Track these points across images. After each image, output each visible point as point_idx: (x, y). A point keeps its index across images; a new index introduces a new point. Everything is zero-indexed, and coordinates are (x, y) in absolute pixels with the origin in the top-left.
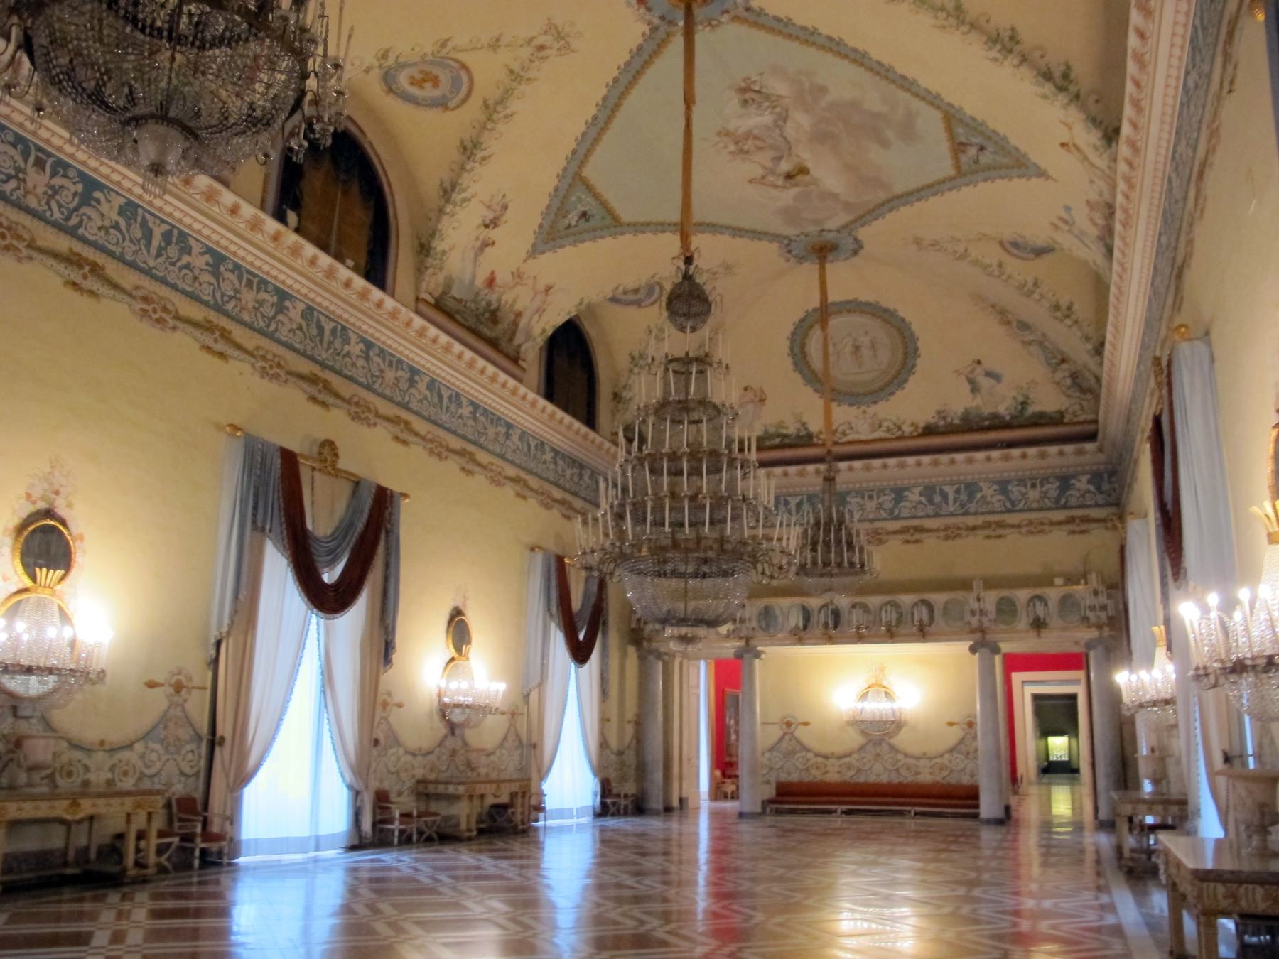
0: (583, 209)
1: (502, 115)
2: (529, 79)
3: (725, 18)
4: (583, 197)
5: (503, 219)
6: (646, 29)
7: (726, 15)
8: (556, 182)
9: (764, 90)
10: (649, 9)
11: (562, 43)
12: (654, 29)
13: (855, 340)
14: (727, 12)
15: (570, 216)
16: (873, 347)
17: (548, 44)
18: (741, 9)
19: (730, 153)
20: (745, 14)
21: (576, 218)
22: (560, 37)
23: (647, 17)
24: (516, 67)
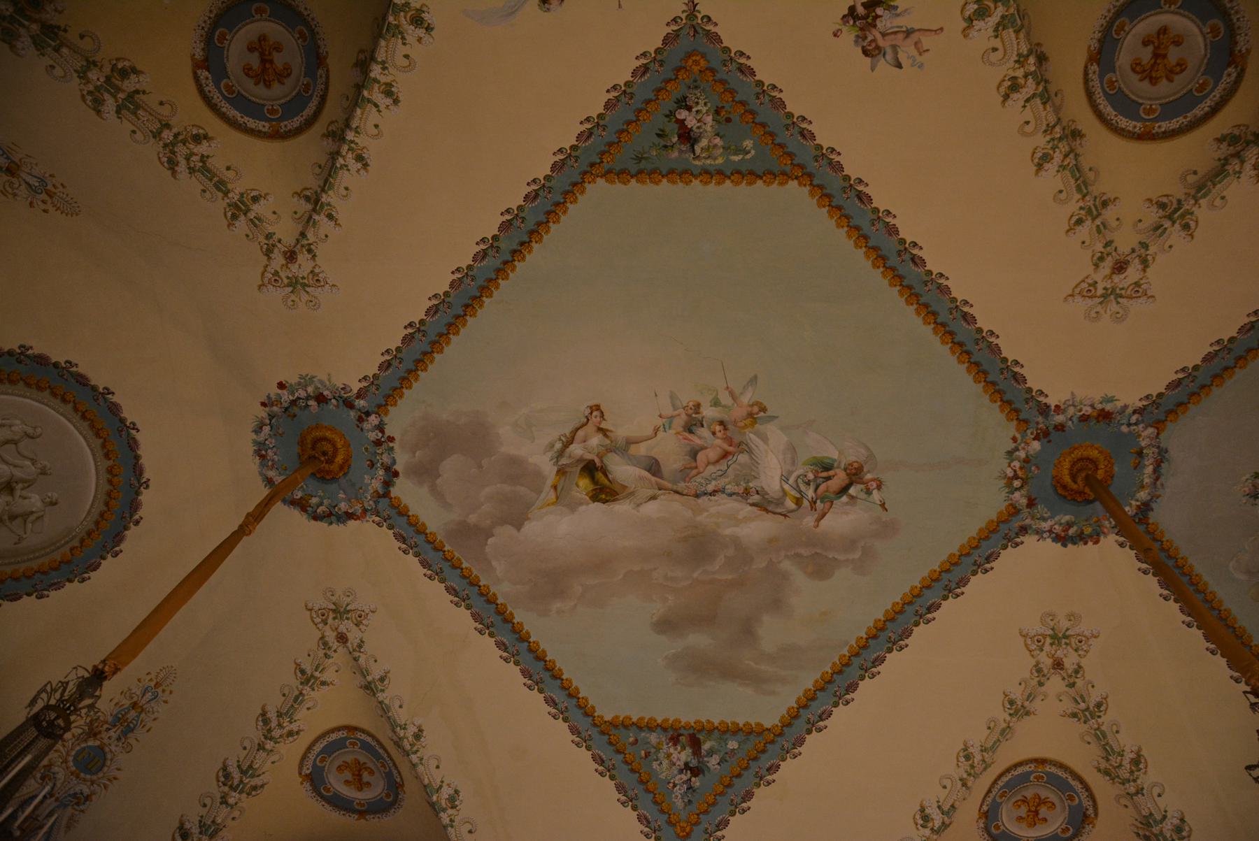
0: (704, 143)
1: (1058, 157)
2: (1080, 222)
3: (1020, 498)
4: (736, 158)
5: (849, 35)
6: (1052, 401)
7: (1024, 501)
8: (824, 140)
9: (844, 499)
10: (1084, 419)
11: (1100, 292)
12: (1044, 410)
13: (28, 483)
14: (1031, 503)
15: (709, 119)
16: (13, 517)
17: (1116, 278)
18: (1028, 522)
19: (698, 406)
20: (1016, 524)
21: (691, 122)
22: (1112, 294)
23: (1071, 411)
24: (1109, 214)
